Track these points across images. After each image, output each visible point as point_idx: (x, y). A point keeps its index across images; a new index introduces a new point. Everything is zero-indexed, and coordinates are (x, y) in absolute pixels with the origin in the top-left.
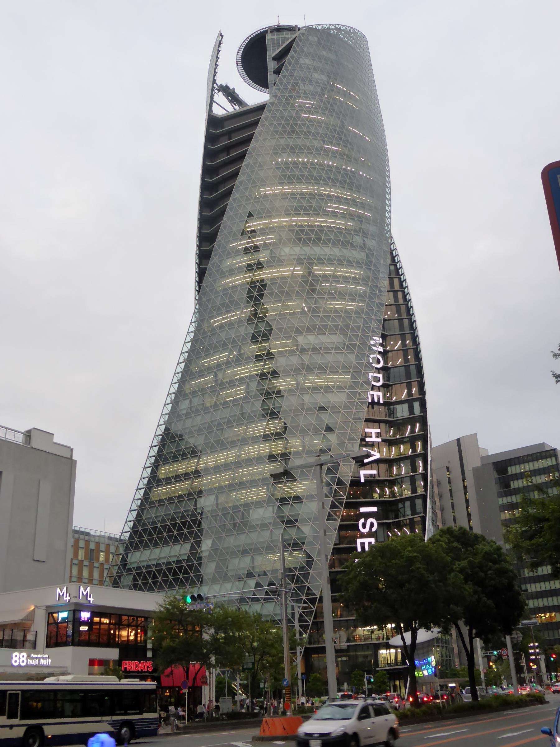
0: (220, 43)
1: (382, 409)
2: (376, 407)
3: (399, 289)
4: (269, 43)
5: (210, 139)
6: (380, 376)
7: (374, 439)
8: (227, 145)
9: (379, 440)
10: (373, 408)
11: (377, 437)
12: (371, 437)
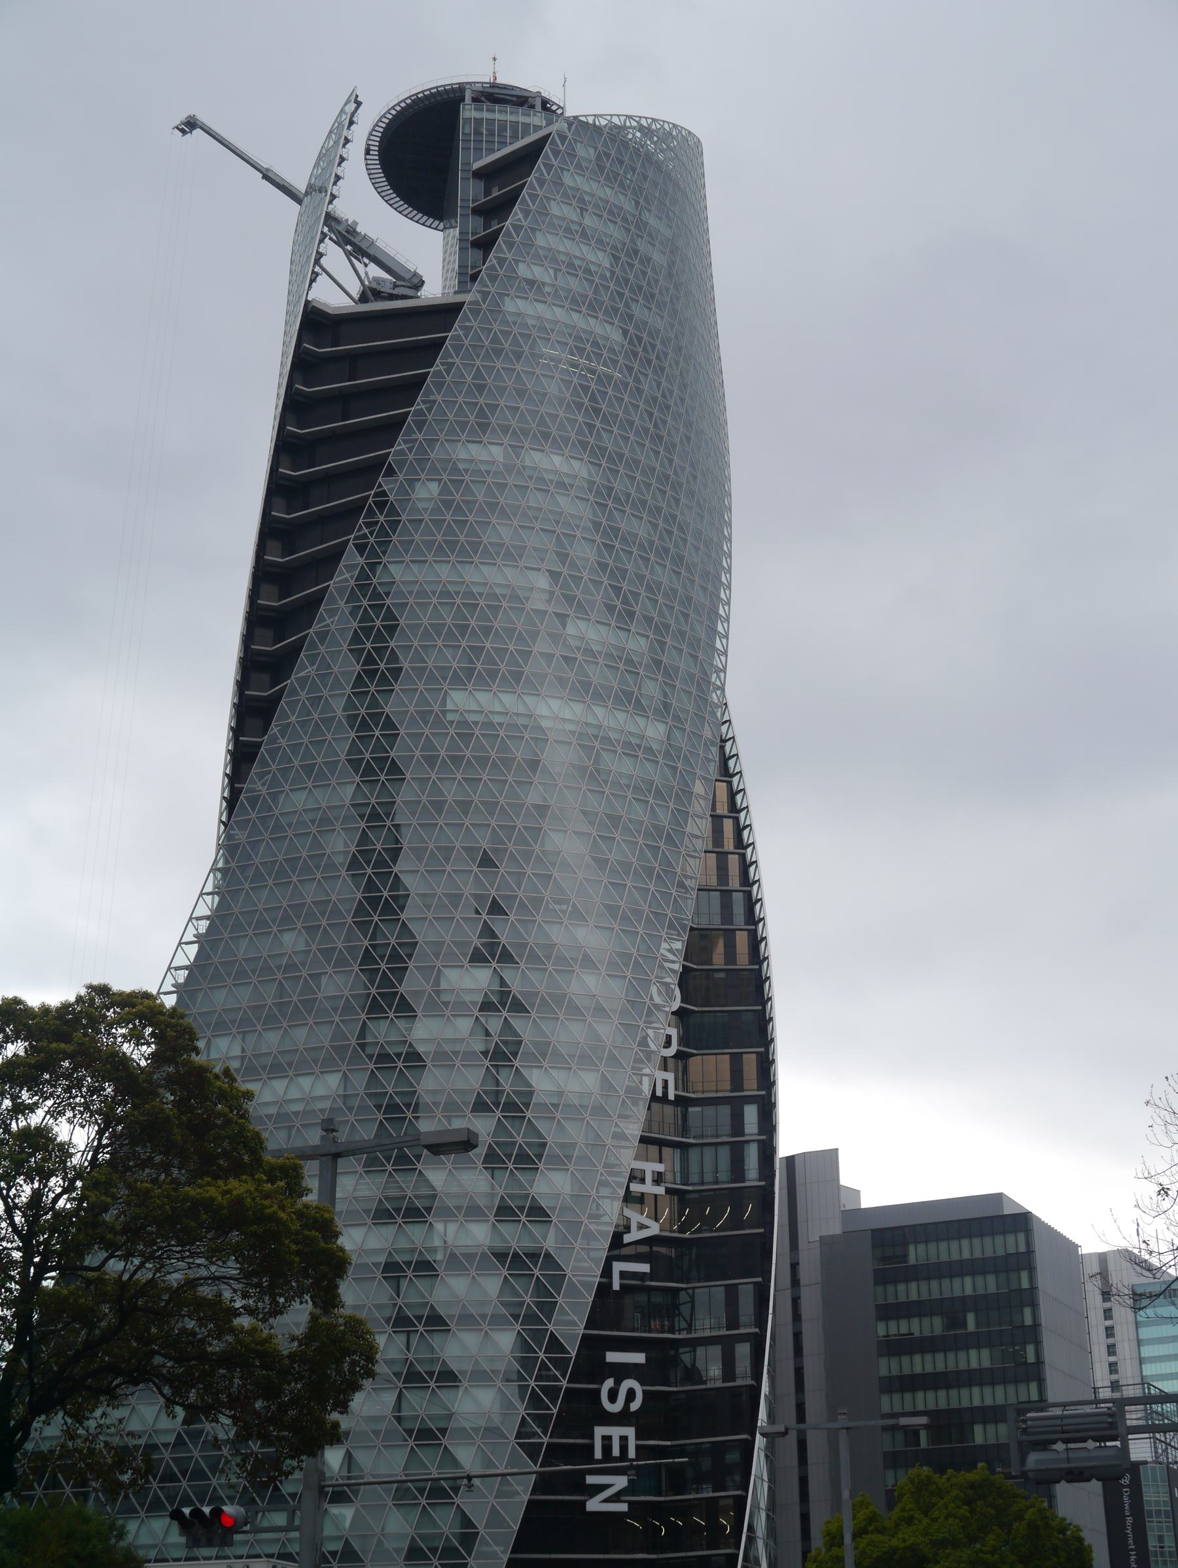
1: (669, 1110)
3: (726, 812)
4: (464, 130)
5: (303, 366)
7: (649, 1188)
9: (660, 1190)
12: (643, 1181)
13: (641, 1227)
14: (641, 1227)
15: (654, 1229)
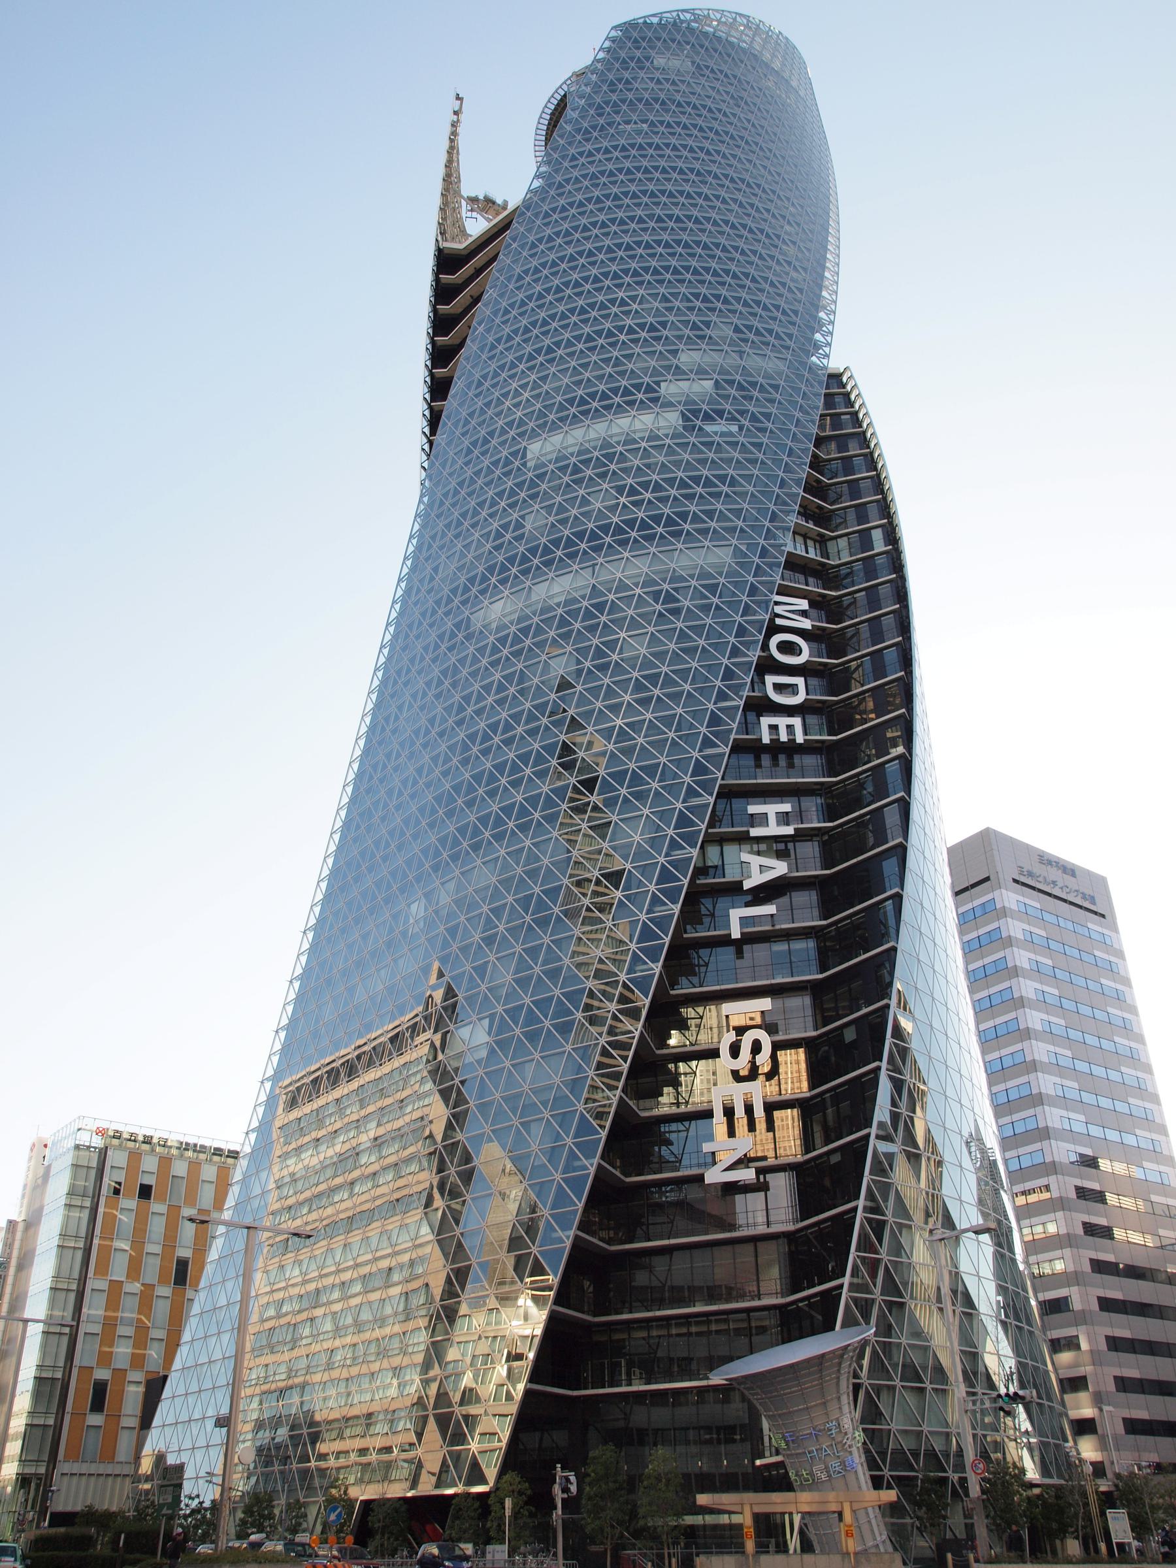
1: (810, 761)
6: (800, 681)
15: (780, 868)
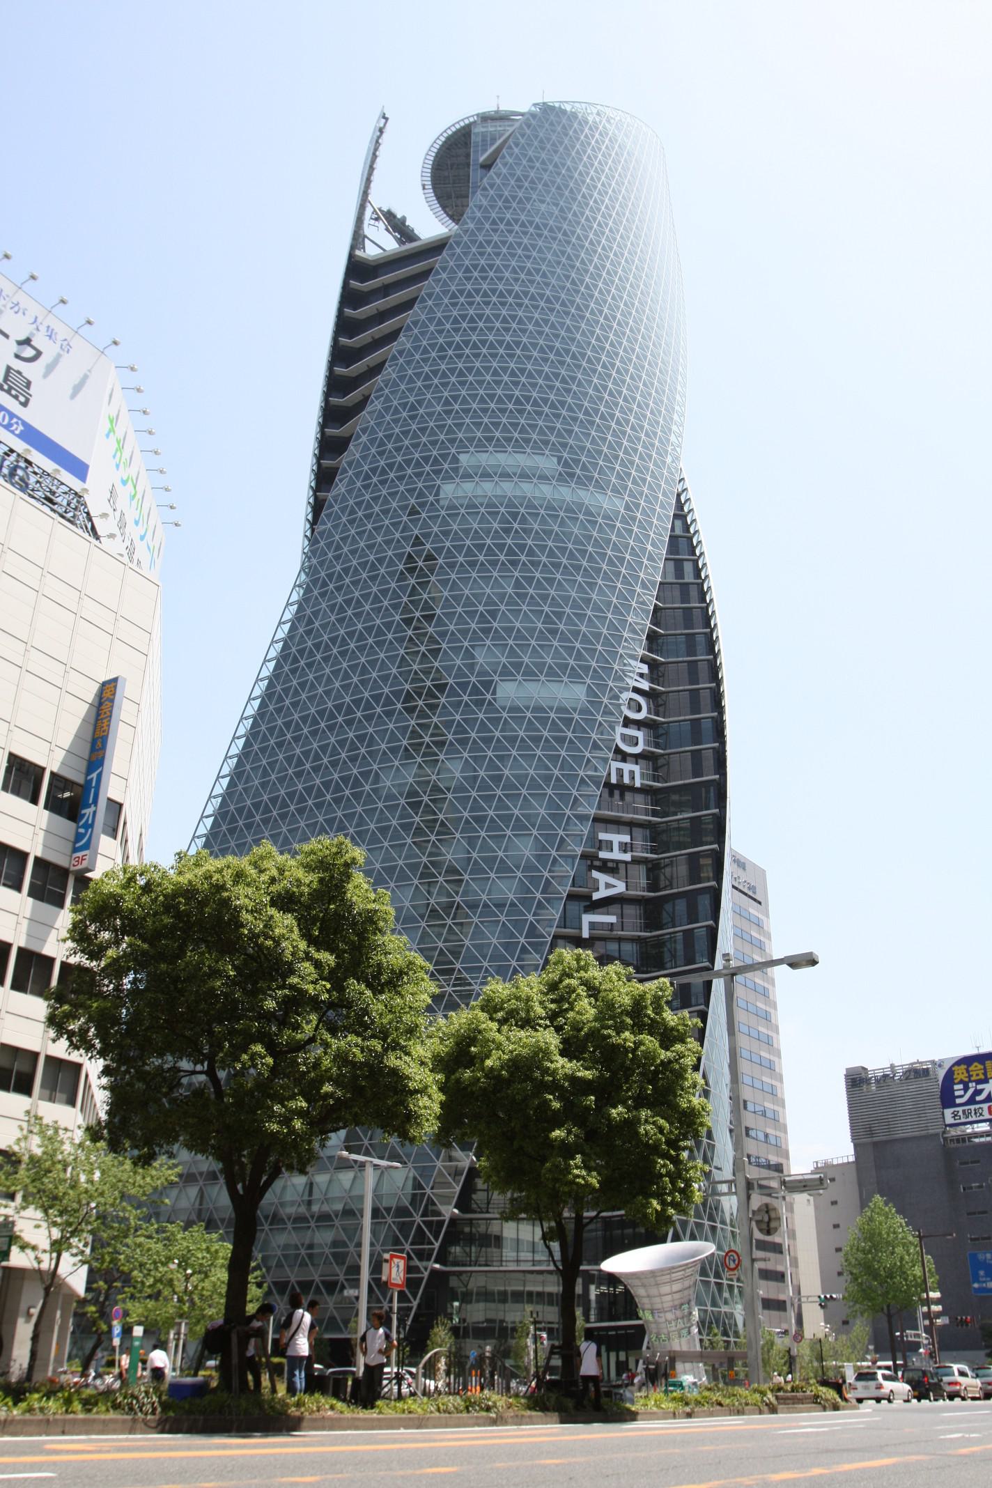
0: (381, 131)
1: (640, 798)
2: (628, 796)
5: (349, 298)
6: (640, 735)
7: (616, 855)
8: (377, 301)
10: (622, 797)
11: (625, 851)
13: (608, 886)
14: (608, 886)
15: (620, 887)
